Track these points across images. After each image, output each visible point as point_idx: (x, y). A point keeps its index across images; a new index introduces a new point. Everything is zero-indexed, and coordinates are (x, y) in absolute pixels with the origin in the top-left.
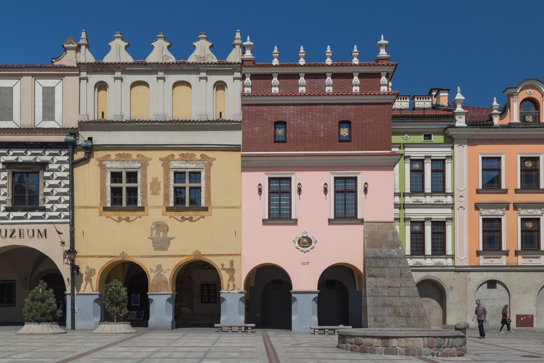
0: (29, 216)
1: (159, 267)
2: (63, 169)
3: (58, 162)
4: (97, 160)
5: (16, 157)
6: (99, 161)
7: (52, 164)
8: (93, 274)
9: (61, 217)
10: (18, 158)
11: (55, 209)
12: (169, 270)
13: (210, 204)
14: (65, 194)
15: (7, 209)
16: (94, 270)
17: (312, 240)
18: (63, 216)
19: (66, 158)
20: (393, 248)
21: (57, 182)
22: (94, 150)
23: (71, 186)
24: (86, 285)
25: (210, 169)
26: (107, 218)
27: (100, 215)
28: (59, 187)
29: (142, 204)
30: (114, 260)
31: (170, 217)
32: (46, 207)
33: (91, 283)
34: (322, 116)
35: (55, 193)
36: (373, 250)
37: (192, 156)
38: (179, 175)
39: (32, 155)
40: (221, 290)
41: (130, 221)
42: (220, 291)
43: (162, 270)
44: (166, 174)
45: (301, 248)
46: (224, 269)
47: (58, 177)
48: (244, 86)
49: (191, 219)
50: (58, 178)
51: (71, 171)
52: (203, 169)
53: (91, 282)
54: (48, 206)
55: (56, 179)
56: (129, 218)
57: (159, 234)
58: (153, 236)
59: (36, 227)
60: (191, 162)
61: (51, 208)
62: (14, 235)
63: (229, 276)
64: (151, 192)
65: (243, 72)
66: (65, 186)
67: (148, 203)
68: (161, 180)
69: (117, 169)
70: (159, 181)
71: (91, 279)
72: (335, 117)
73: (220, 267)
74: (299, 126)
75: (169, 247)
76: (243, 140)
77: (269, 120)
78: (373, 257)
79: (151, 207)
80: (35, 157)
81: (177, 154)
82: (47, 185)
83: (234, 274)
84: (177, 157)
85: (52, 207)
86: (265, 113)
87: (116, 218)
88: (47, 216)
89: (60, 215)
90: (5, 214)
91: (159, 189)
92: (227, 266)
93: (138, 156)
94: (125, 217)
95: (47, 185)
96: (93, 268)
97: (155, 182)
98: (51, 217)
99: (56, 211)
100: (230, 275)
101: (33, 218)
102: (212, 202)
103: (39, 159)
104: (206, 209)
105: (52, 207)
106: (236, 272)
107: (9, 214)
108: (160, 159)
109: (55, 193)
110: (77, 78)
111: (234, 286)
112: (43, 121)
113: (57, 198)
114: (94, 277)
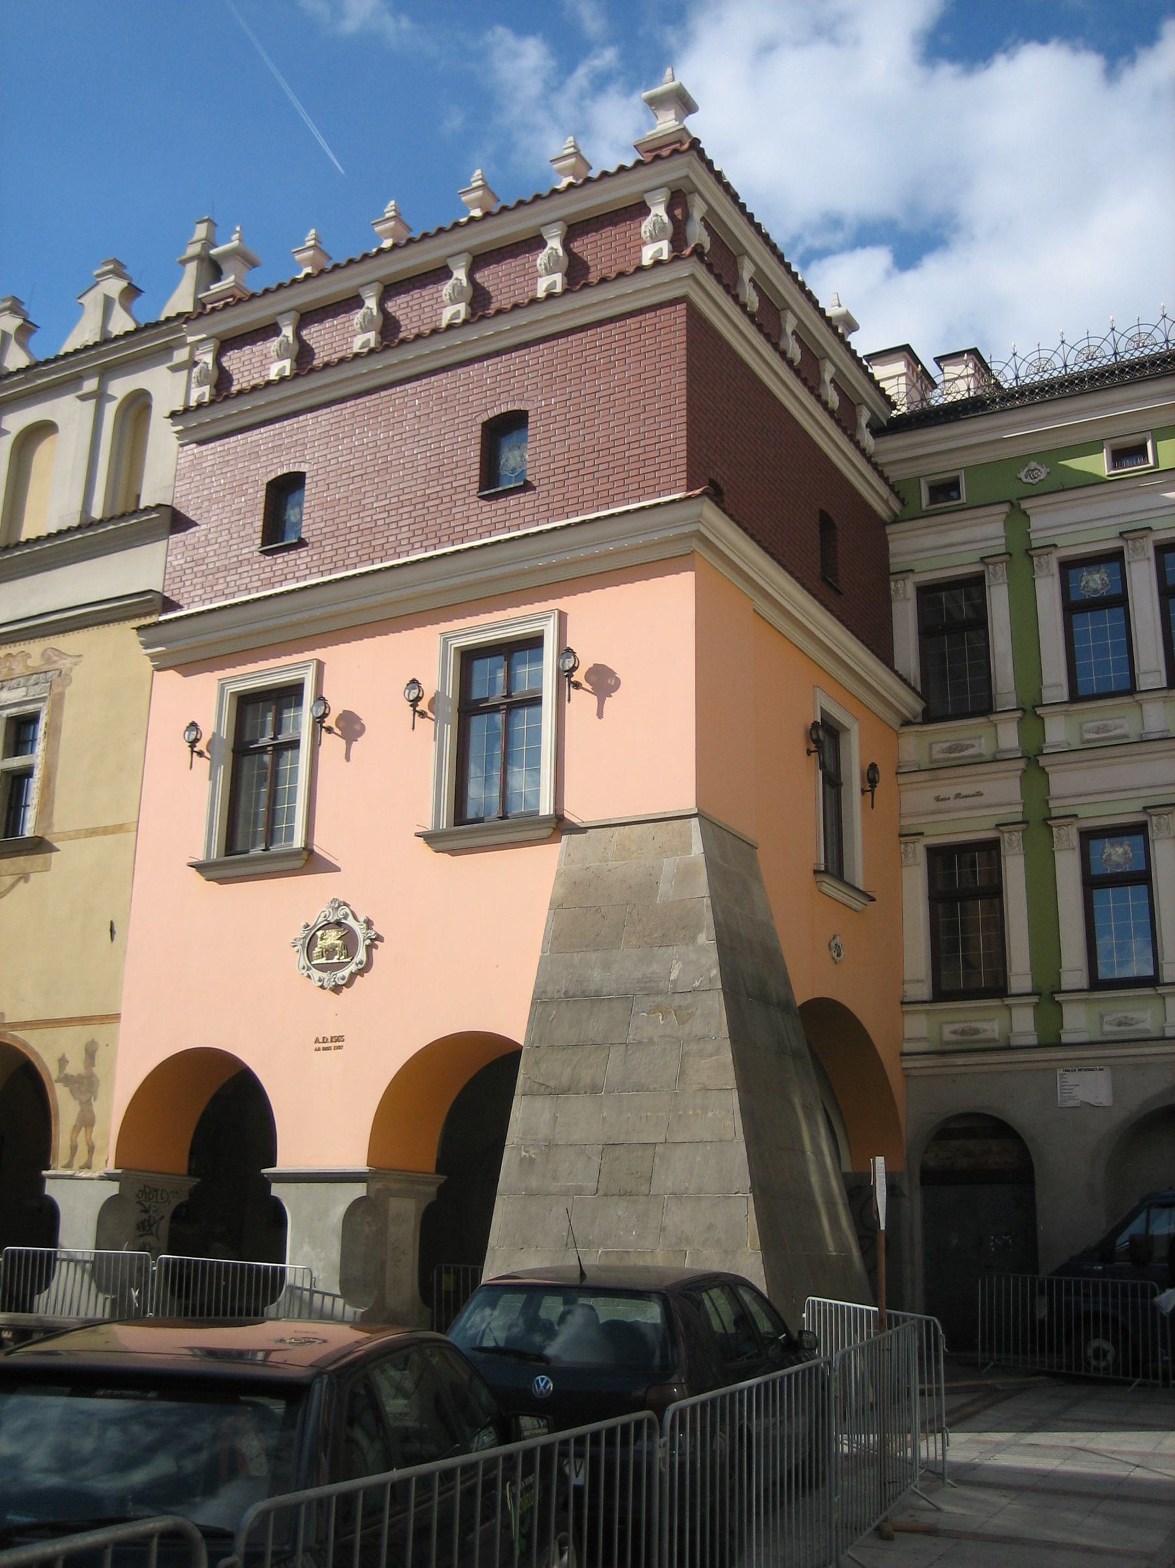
17: (361, 937)
20: (666, 941)
36: (576, 958)
40: (48, 1168)
42: (44, 1173)
45: (316, 974)
46: (66, 1080)
52: (43, 699)
63: (79, 1109)
78: (566, 993)
83: (95, 1100)
92: (75, 1067)
100: (81, 1103)
104: (40, 846)
106: (102, 1090)
111: (91, 1149)
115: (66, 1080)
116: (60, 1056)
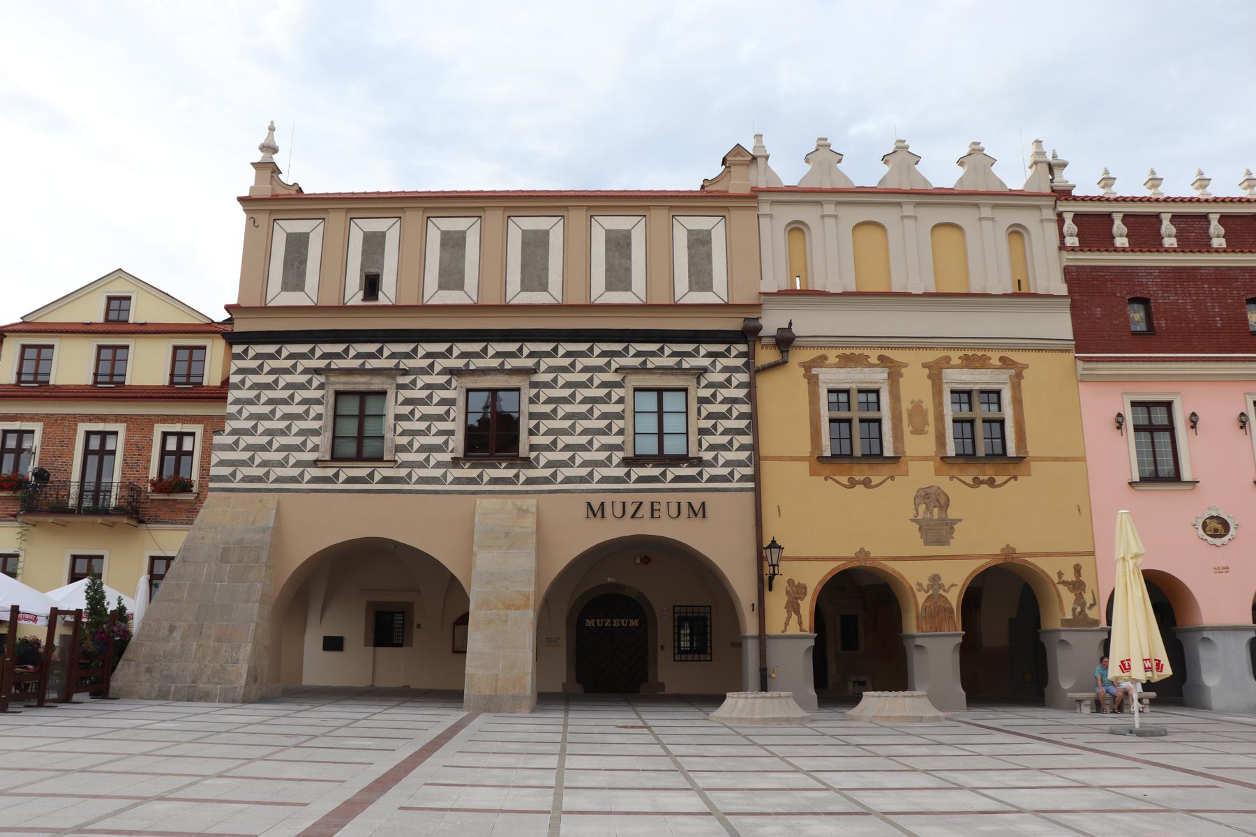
0: (670, 476)
1: (935, 579)
2: (735, 382)
3: (726, 369)
4: (800, 366)
5: (643, 359)
6: (804, 367)
7: (713, 372)
8: (802, 596)
9: (733, 478)
10: (645, 362)
11: (721, 461)
12: (956, 585)
13: (1027, 452)
14: (740, 432)
15: (627, 462)
16: (805, 588)
18: (737, 476)
19: (740, 362)
21: (724, 408)
22: (794, 347)
23: (752, 416)
24: (789, 617)
25: (1019, 385)
26: (826, 479)
27: (813, 473)
28: (729, 419)
29: (895, 452)
30: (844, 565)
31: (951, 479)
32: (704, 459)
33: (798, 612)
34: (1214, 289)
35: (720, 429)
37: (986, 359)
38: (963, 395)
39: (674, 354)
41: (872, 487)
43: (941, 586)
44: (938, 393)
46: (1064, 583)
47: (725, 398)
48: (1062, 237)
49: (991, 483)
50: (726, 400)
51: (751, 386)
53: (799, 612)
54: (708, 456)
55: (721, 403)
56: (871, 481)
57: (932, 513)
58: (920, 517)
59: (684, 498)
60: (982, 371)
61: (713, 459)
62: (638, 515)
64: (911, 428)
65: (1060, 209)
66: (741, 416)
67: (906, 450)
68: (928, 405)
69: (839, 383)
70: (924, 406)
71: (798, 605)
72: (1237, 291)
73: (1056, 579)
74: (1174, 307)
75: (953, 538)
76: (1074, 332)
77: (1119, 295)
79: (913, 459)
80: (679, 358)
81: (955, 357)
82: (704, 414)
83: (1084, 593)
84: (955, 360)
85: (716, 458)
86: (1108, 283)
87: (844, 480)
88: (706, 476)
89: (731, 473)
90: (621, 472)
91: (926, 423)
92: (1070, 576)
93: (881, 358)
94: (862, 478)
95: (704, 414)
96: (801, 583)
97: (917, 409)
98: (712, 479)
99: (724, 466)
100: (1075, 595)
101: (677, 479)
102: (1028, 450)
103: (688, 363)
105: (716, 458)
107: (629, 471)
108: (925, 366)
109: (720, 429)
110: (754, 214)
112: (690, 291)
113: (724, 440)
114: (804, 601)
115: (1064, 583)
116: (1058, 571)
